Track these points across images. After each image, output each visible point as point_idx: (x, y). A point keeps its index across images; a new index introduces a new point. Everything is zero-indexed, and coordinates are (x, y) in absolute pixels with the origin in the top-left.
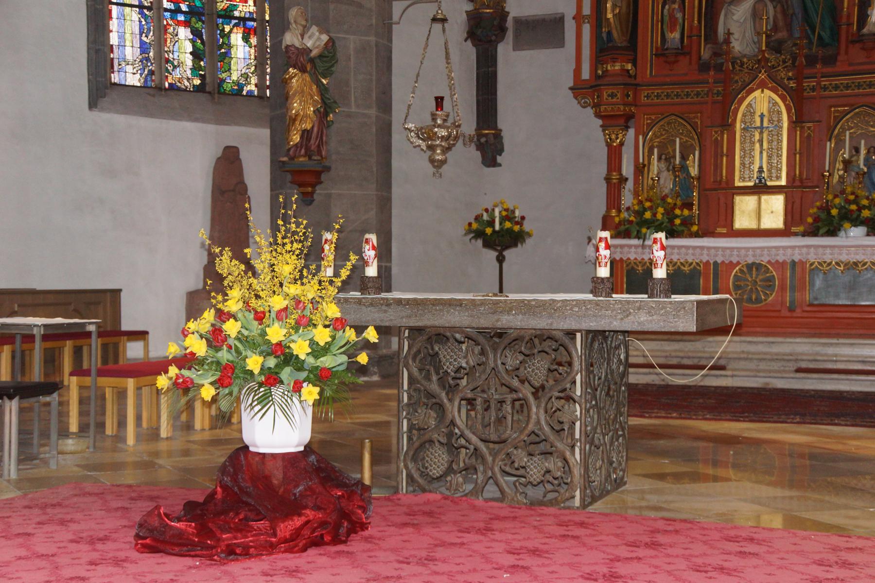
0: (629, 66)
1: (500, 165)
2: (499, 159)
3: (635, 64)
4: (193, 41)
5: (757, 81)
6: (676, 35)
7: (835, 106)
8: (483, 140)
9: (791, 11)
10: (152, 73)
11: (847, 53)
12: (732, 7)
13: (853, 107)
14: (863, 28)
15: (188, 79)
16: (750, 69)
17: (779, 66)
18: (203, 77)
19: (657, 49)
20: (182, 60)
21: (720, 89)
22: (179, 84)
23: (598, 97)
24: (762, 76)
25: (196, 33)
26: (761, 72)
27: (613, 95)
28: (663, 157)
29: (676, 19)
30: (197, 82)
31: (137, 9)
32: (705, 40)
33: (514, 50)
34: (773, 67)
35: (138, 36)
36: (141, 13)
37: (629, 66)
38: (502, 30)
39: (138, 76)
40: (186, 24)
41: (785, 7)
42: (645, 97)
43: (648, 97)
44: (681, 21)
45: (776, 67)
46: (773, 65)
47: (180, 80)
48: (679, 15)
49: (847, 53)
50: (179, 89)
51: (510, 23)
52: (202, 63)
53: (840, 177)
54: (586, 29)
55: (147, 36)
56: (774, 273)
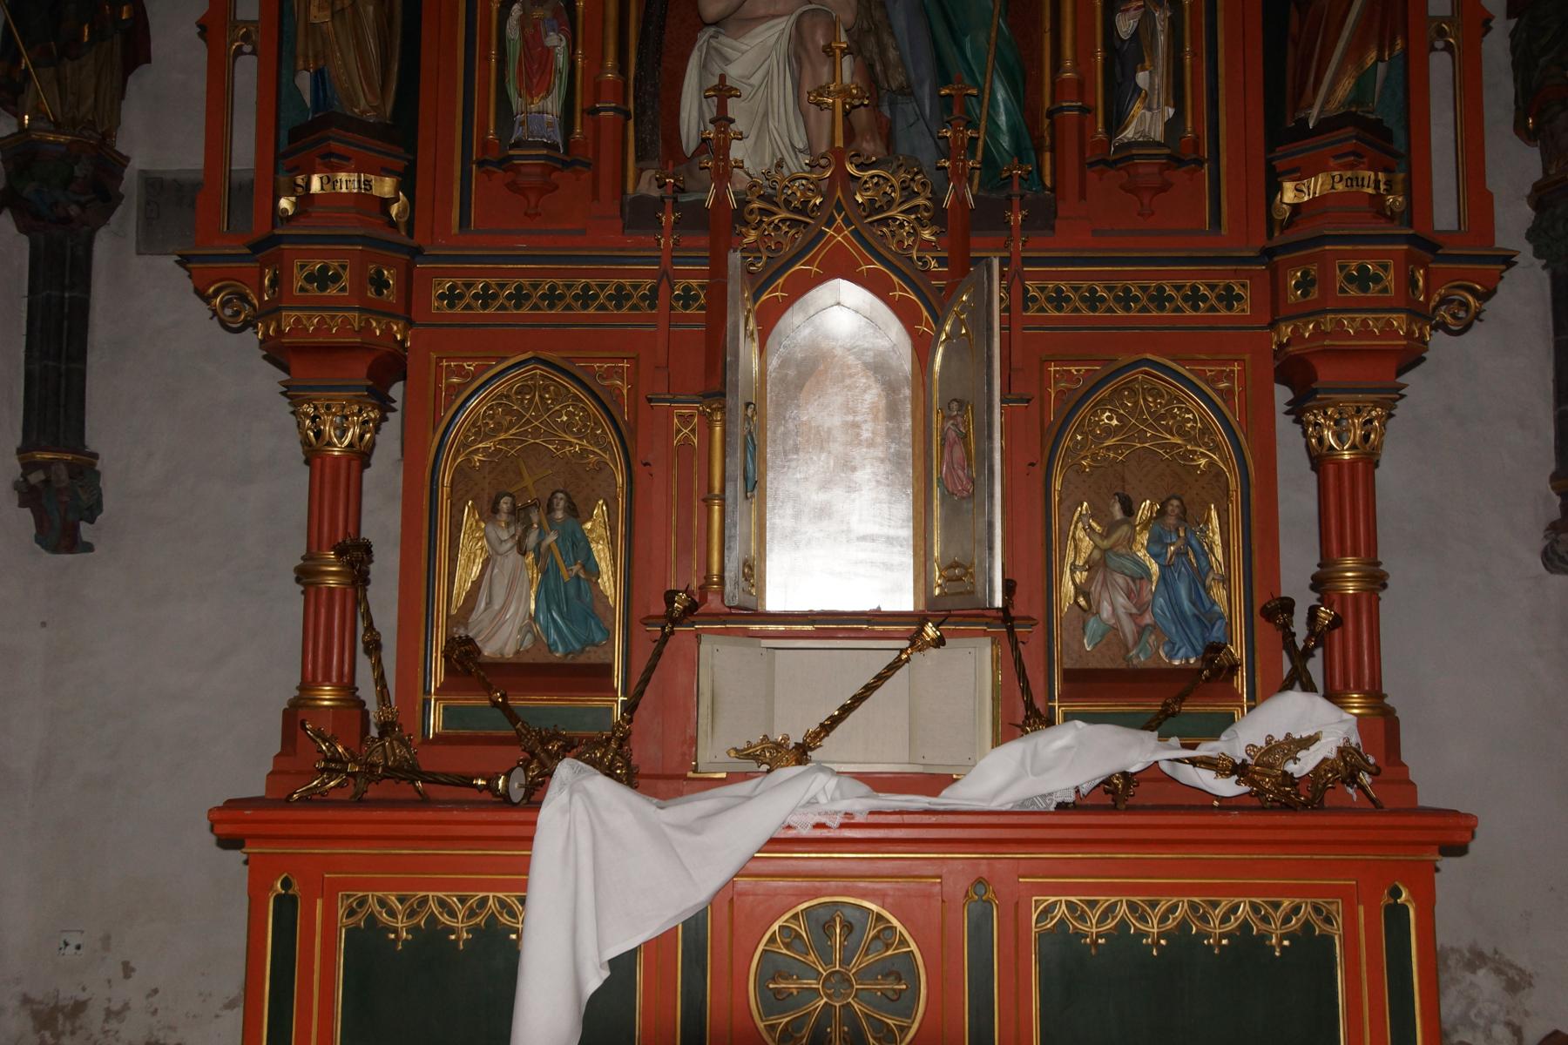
0: (385, 187)
1: (89, 548)
2: (86, 531)
3: (407, 184)
5: (820, 251)
6: (552, 105)
7: (1058, 362)
8: (36, 477)
9: (897, 80)
11: (1082, 195)
12: (722, 39)
13: (1114, 367)
14: (1126, 128)
16: (796, 210)
17: (890, 203)
19: (485, 145)
21: (694, 282)
23: (273, 283)
24: (839, 236)
26: (830, 222)
27: (322, 279)
28: (505, 504)
29: (549, 52)
32: (638, 159)
33: (139, 253)
34: (872, 207)
37: (385, 187)
38: (104, 196)
41: (878, 68)
42: (442, 297)
43: (452, 297)
44: (561, 60)
45: (881, 210)
46: (872, 201)
48: (556, 42)
49: (1082, 195)
51: (130, 184)
53: (1080, 590)
54: (246, 74)
56: (913, 947)
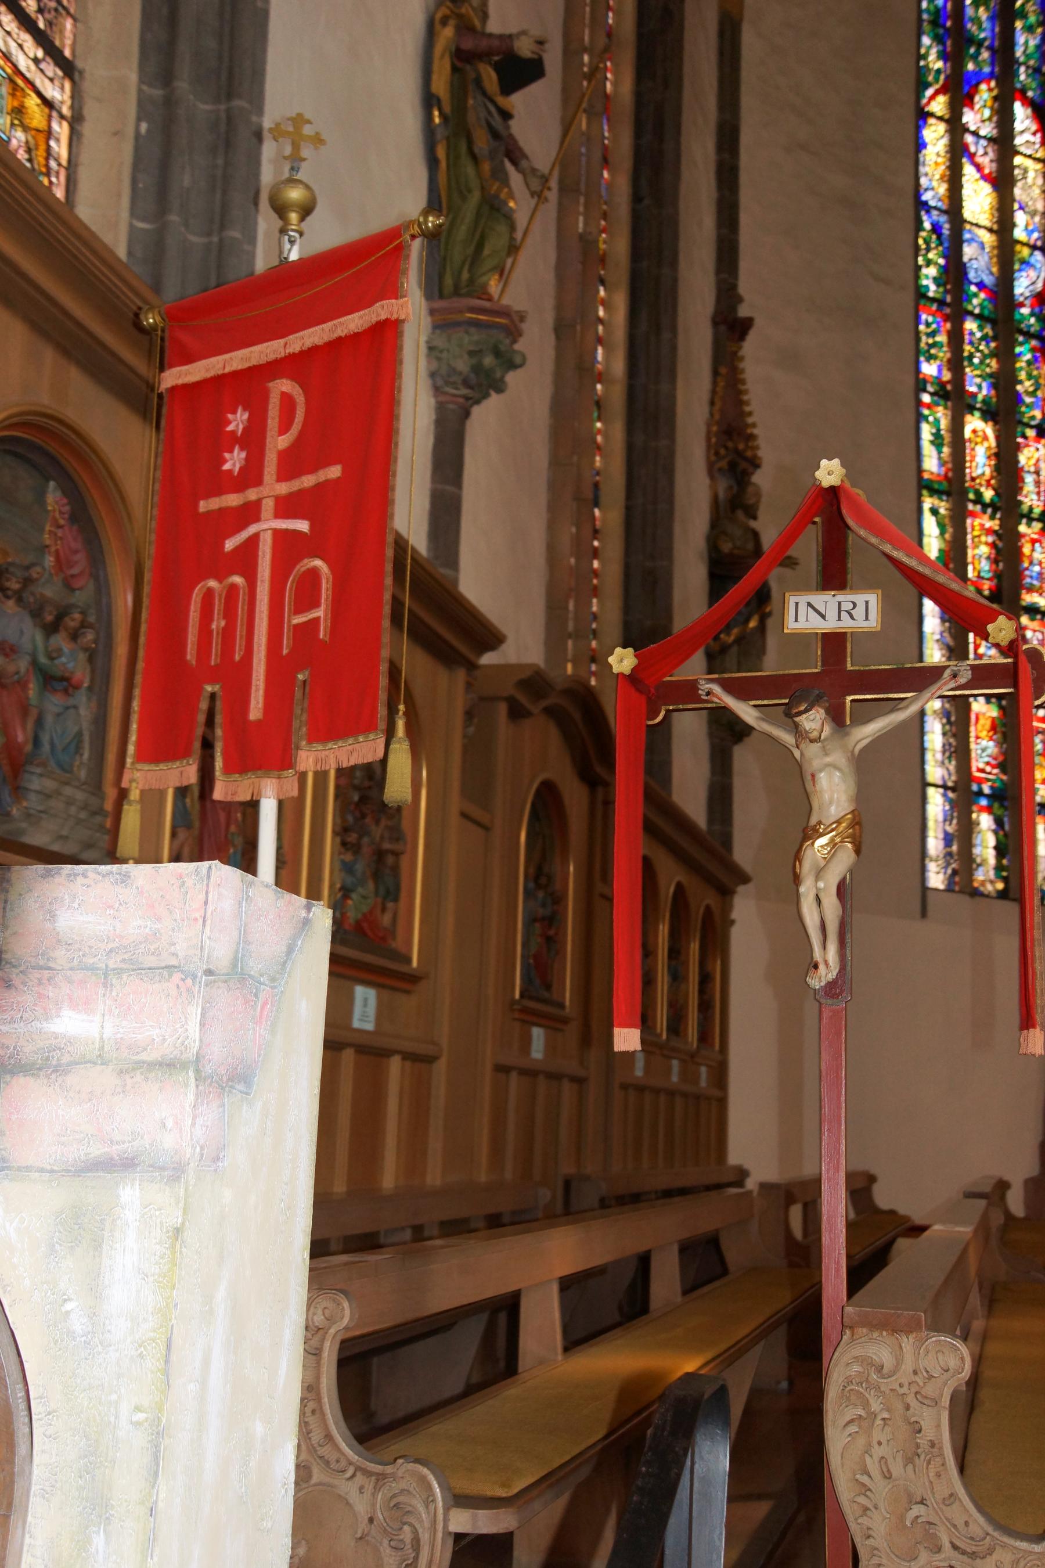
4: (995, 832)
10: (955, 872)
15: (992, 882)
18: (1005, 880)
20: (985, 856)
22: (982, 889)
25: (999, 822)
30: (1000, 886)
31: (941, 790)
35: (941, 825)
36: (944, 795)
39: (941, 876)
40: (989, 809)
47: (983, 883)
50: (982, 895)
52: (1005, 862)
55: (950, 824)
